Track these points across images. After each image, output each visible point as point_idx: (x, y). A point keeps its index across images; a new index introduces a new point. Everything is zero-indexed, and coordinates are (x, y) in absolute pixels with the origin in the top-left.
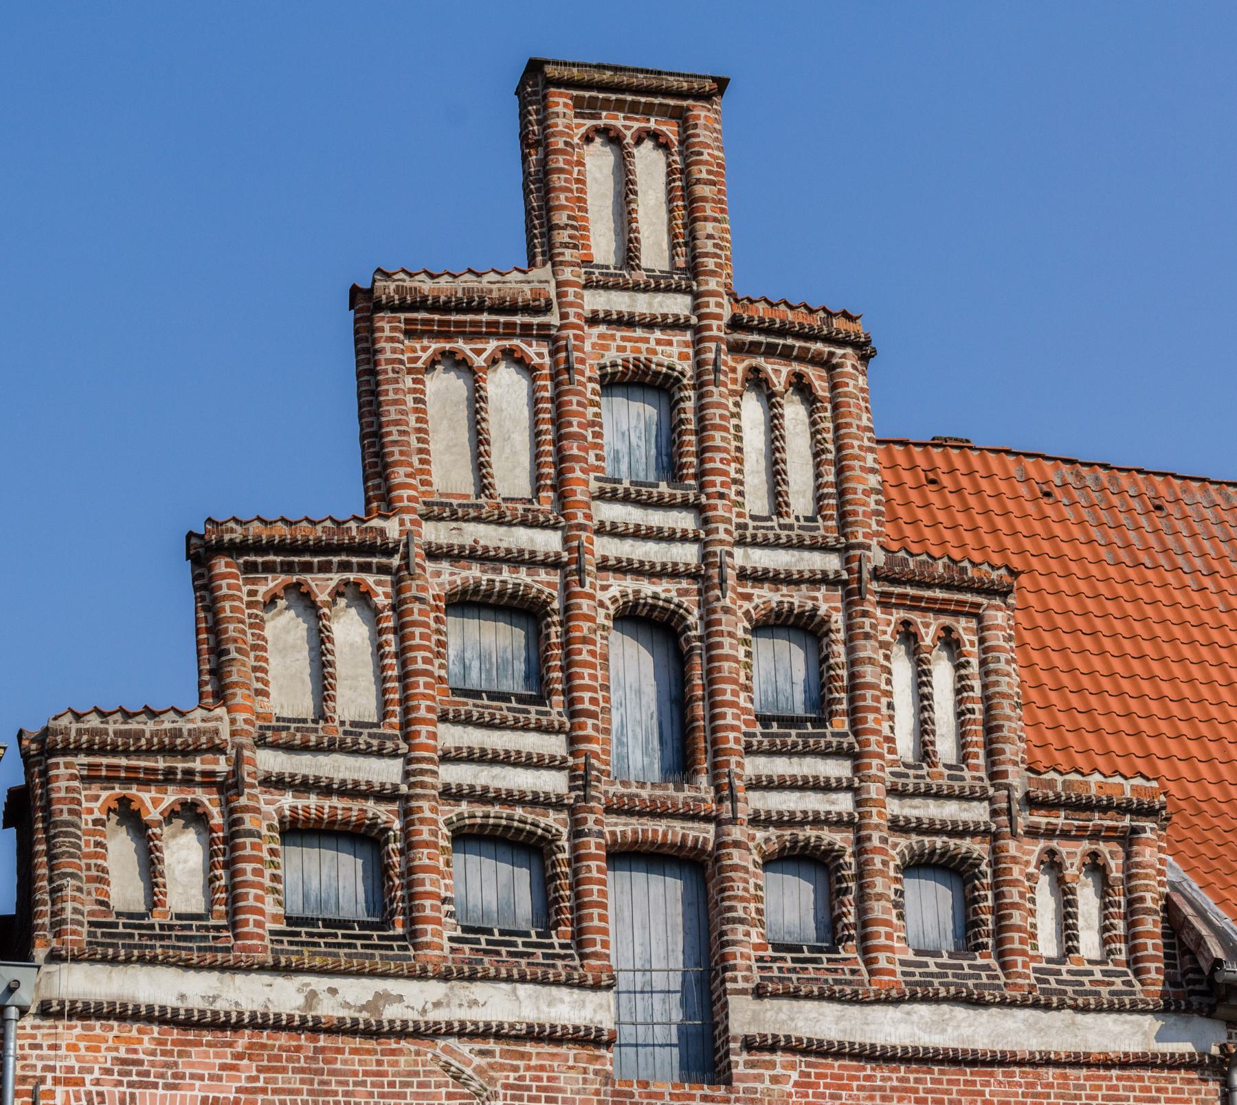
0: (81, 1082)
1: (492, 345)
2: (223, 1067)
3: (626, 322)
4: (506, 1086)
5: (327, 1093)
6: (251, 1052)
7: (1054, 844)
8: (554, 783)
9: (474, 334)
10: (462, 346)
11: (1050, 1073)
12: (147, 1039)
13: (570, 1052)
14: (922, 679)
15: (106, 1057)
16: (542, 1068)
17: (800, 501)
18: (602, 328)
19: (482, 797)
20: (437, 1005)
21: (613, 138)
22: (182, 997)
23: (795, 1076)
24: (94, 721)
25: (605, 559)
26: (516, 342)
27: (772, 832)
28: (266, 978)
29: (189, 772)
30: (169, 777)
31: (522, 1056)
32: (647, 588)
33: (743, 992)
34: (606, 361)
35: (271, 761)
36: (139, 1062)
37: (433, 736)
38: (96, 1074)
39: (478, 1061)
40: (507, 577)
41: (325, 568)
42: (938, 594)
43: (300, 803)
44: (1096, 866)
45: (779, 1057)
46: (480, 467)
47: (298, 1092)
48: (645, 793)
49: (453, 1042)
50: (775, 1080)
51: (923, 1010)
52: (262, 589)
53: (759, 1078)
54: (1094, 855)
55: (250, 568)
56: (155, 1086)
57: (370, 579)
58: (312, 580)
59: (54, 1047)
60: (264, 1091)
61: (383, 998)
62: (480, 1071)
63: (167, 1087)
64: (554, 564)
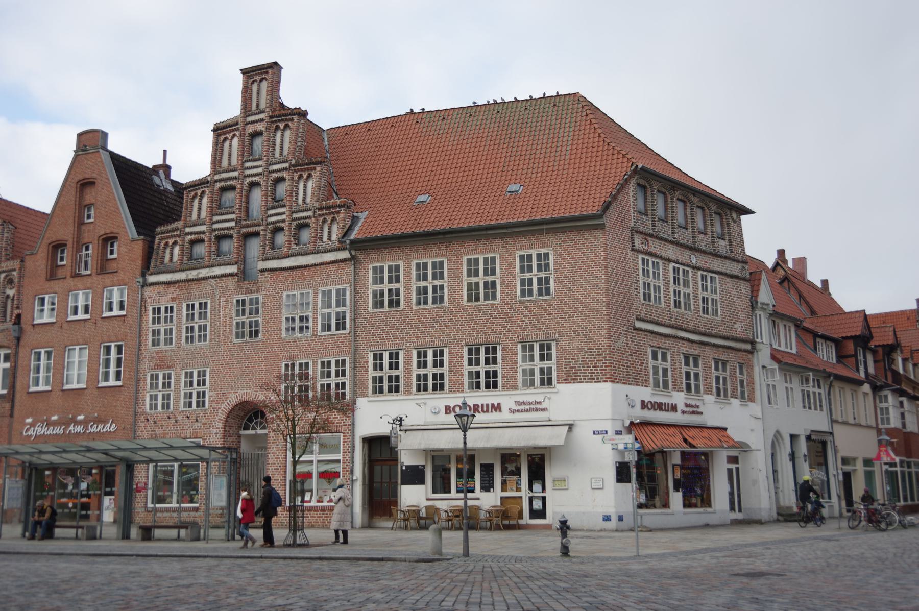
3: (253, 122)
7: (326, 217)
8: (233, 224)
9: (229, 132)
11: (318, 268)
12: (162, 288)
13: (230, 278)
15: (156, 292)
23: (269, 276)
28: (180, 273)
32: (254, 179)
35: (188, 230)
40: (229, 183)
41: (199, 189)
42: (306, 167)
45: (266, 273)
49: (211, 280)
50: (265, 277)
53: (262, 278)
61: (199, 273)
64: (235, 178)
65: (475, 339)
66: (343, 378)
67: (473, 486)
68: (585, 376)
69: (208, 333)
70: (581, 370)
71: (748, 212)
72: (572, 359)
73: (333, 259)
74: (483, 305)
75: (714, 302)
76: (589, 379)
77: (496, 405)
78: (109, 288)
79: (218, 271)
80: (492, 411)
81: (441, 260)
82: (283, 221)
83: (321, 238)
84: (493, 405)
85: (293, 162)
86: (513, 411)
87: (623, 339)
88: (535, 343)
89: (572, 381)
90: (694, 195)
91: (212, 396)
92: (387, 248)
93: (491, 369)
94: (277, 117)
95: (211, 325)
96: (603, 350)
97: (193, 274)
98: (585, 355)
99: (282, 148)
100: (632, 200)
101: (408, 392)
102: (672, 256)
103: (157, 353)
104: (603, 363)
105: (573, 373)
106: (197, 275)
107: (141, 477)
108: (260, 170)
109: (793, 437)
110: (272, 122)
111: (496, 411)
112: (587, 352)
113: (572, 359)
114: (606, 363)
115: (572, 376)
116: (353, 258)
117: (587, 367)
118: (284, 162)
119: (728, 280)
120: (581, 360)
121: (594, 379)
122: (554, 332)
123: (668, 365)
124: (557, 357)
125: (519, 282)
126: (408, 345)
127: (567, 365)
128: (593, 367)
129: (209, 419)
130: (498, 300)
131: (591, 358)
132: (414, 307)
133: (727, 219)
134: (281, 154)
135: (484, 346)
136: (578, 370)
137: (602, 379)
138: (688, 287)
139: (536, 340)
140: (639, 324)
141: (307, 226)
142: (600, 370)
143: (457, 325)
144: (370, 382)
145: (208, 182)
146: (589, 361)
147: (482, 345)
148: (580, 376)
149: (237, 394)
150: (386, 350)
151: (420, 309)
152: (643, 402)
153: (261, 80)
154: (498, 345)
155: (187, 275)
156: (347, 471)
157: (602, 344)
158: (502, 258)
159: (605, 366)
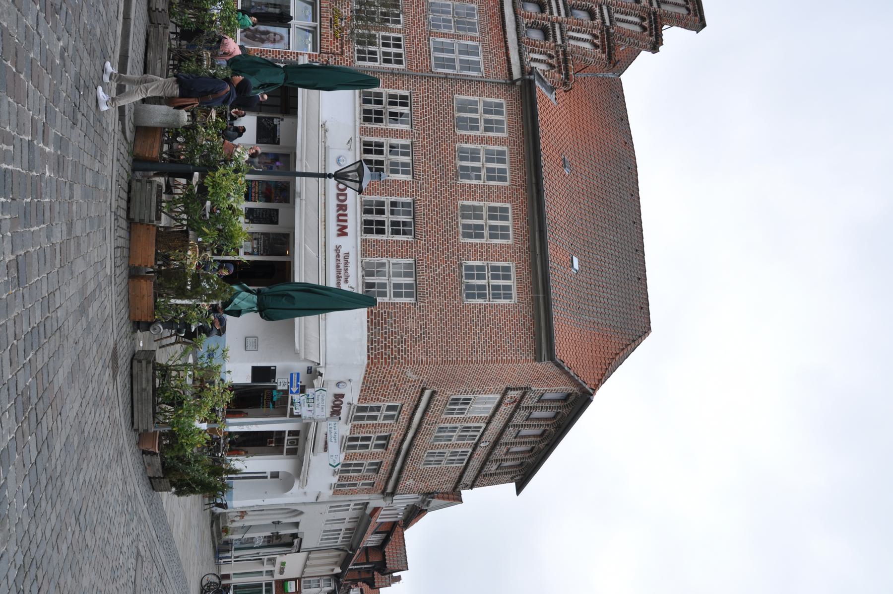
11: (503, 44)
42: (606, 43)
65: (420, 210)
66: (382, 60)
67: (253, 199)
68: (375, 335)
70: (382, 330)
71: (519, 490)
72: (395, 320)
73: (512, 61)
74: (457, 223)
75: (439, 462)
76: (372, 338)
77: (345, 231)
80: (338, 225)
81: (508, 179)
82: (551, 13)
83: (534, 51)
84: (346, 227)
85: (612, 31)
86: (338, 249)
87: (414, 377)
88: (414, 279)
89: (370, 320)
90: (547, 445)
93: (386, 227)
94: (654, 19)
96: (404, 356)
98: (398, 335)
100: (557, 388)
101: (363, 131)
102: (491, 426)
104: (389, 356)
105: (379, 320)
109: (297, 524)
110: (649, 14)
111: (339, 230)
112: (402, 338)
113: (395, 320)
114: (389, 359)
115: (375, 319)
116: (513, 83)
117: (385, 338)
118: (611, 21)
119: (458, 474)
120: (394, 330)
121: (372, 344)
122: (426, 301)
123: (380, 421)
124: (397, 303)
125: (507, 265)
126: (418, 135)
127: (388, 314)
128: (385, 344)
130: (462, 240)
131: (395, 342)
132: (457, 145)
133: (516, 471)
134: (618, 20)
135: (412, 220)
136: (382, 327)
137: (372, 353)
138: (458, 440)
139: (417, 280)
140: (427, 393)
141: (546, 38)
142: (382, 352)
143: (436, 192)
146: (392, 339)
147: (414, 219)
148: (375, 328)
150: (411, 110)
151: (455, 151)
152: (342, 396)
153: (688, 9)
154: (413, 237)
156: (276, 56)
157: (411, 354)
158: (508, 246)
159: (385, 358)
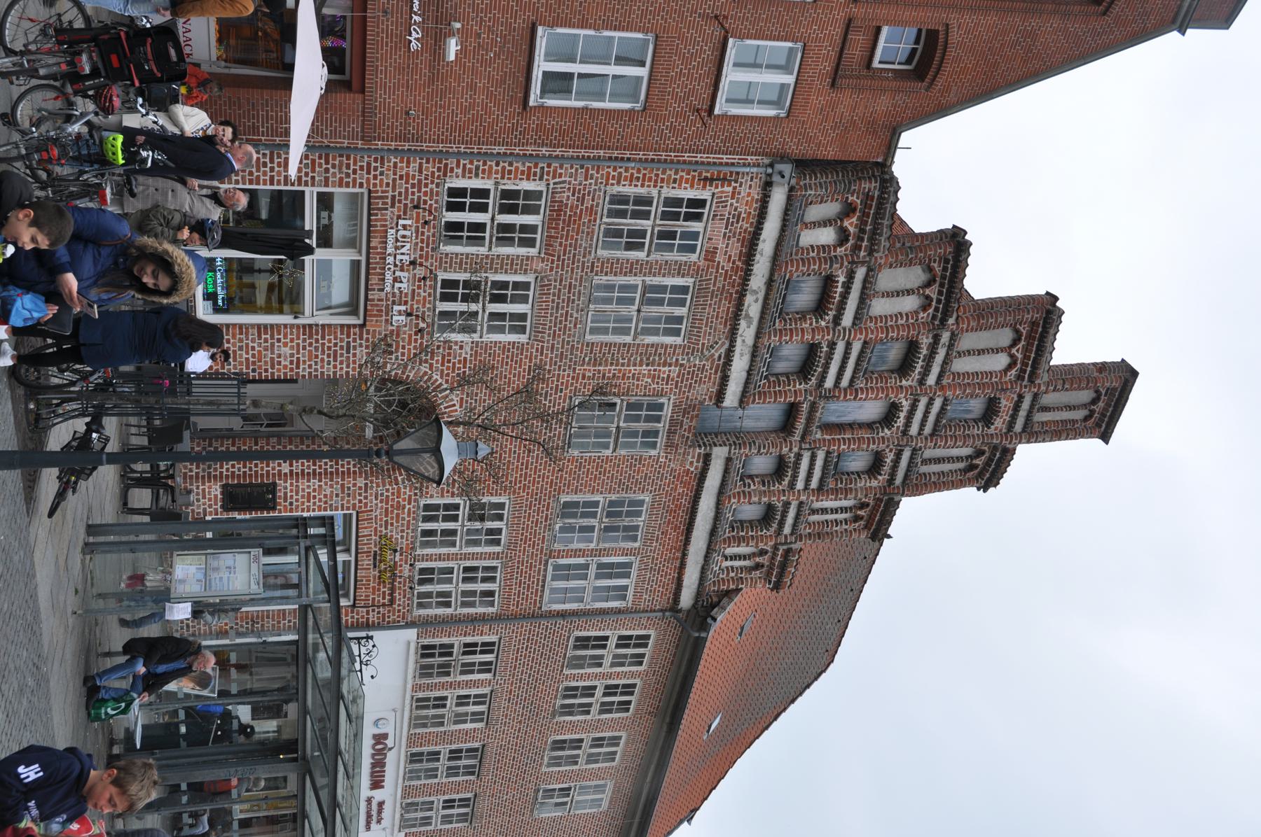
0: (732, 198)
1: (1019, 356)
2: (730, 256)
3: (1017, 408)
4: (704, 365)
5: (712, 297)
6: (735, 269)
9: (1026, 350)
10: (1023, 343)
11: (679, 555)
14: (843, 510)
15: (742, 209)
16: (710, 379)
17: (924, 469)
18: (1016, 399)
19: (829, 357)
20: (744, 341)
21: (1095, 401)
22: (764, 241)
23: (692, 469)
24: (892, 199)
25: (919, 401)
26: (1019, 366)
27: (792, 460)
28: (767, 275)
29: (862, 240)
30: (862, 231)
31: (716, 372)
32: (902, 415)
33: (730, 452)
34: (1002, 400)
35: (861, 273)
36: (738, 222)
37: (860, 339)
38: (735, 204)
39: (717, 355)
41: (940, 293)
43: (840, 285)
44: (758, 566)
45: (700, 464)
46: (969, 353)
47: (714, 286)
48: (818, 414)
49: (727, 346)
50: (692, 463)
51: (712, 514)
52: (936, 265)
53: (693, 457)
54: (763, 566)
55: (947, 261)
56: (726, 228)
57: (931, 311)
58: (936, 287)
59: (750, 186)
60: (717, 272)
62: (713, 355)
63: (725, 234)
64: (921, 382)
69: (610, 338)
78: (799, 55)
79: (739, 365)
82: (792, 485)
84: (383, 781)
86: (369, 800)
91: (461, 348)
92: (677, 648)
95: (625, 345)
97: (753, 307)
99: (938, 461)
101: (416, 688)
103: (591, 210)
106: (747, 316)
107: (272, 169)
108: (914, 430)
129: (409, 344)
144: (445, 640)
145: (943, 321)
149: (457, 407)
150: (497, 657)
155: (755, 292)
